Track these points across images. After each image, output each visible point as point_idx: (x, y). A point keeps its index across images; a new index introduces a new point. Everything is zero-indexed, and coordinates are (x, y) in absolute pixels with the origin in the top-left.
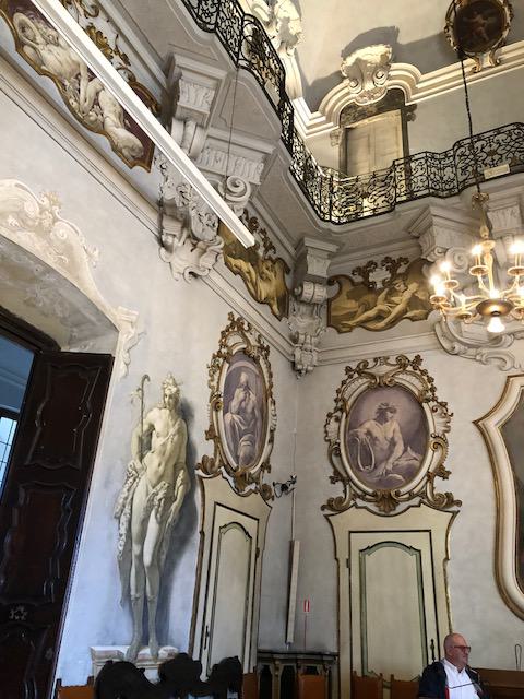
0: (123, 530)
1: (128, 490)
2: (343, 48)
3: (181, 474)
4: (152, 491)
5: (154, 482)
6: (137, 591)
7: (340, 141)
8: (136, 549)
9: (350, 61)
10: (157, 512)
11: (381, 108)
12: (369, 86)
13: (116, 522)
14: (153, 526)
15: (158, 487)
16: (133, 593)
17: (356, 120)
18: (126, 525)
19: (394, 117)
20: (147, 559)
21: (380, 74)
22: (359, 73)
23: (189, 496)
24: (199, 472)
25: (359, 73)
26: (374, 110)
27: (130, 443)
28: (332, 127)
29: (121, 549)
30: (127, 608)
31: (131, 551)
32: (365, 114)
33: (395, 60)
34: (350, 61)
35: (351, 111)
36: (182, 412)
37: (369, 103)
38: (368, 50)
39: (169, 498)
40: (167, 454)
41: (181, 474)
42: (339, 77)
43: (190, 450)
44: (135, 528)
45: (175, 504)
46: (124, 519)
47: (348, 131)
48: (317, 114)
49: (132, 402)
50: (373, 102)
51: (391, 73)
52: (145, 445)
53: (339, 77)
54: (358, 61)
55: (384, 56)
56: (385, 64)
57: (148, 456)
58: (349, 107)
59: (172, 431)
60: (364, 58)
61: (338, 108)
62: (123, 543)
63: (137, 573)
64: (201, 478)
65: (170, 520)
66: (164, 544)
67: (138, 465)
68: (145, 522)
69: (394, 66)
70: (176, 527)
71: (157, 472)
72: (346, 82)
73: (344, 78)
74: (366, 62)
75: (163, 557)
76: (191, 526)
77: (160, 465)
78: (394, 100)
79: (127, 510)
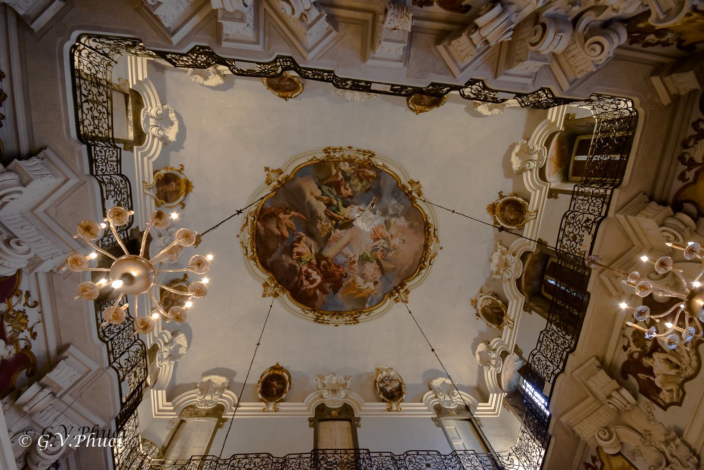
2: (205, 371)
7: (173, 427)
9: (205, 379)
11: (208, 414)
12: (208, 398)
17: (190, 416)
19: (213, 421)
21: (217, 393)
22: (206, 388)
25: (206, 388)
26: (204, 414)
28: (174, 416)
32: (197, 414)
33: (228, 388)
34: (205, 379)
35: (191, 409)
37: (203, 408)
38: (217, 377)
42: (194, 386)
47: (182, 421)
48: (170, 404)
50: (206, 408)
51: (224, 395)
53: (194, 386)
54: (209, 381)
55: (223, 384)
56: (222, 389)
58: (191, 406)
60: (213, 381)
61: (183, 406)
69: (227, 391)
72: (197, 390)
73: (197, 387)
74: (213, 383)
78: (218, 411)
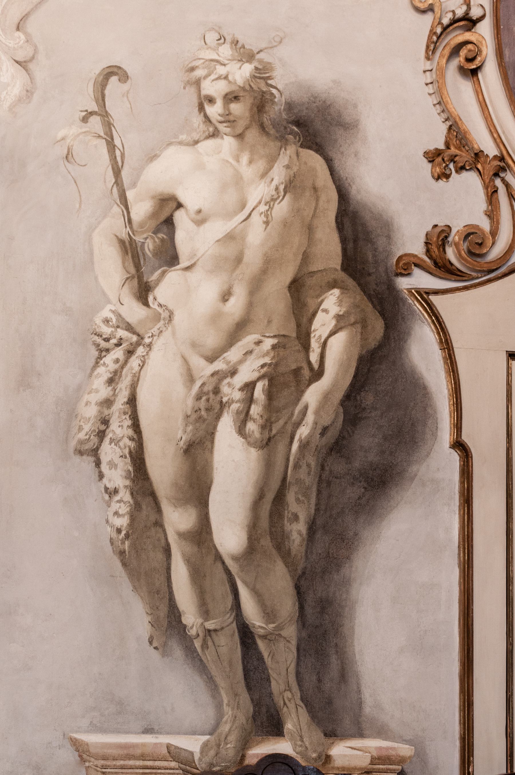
0: (117, 476)
1: (111, 381)
3: (331, 305)
4: (205, 370)
5: (212, 340)
6: (205, 613)
8: (178, 519)
10: (243, 420)
13: (86, 463)
14: (235, 465)
15: (234, 355)
16: (191, 617)
18: (125, 466)
20: (230, 536)
23: (378, 365)
24: (421, 280)
27: (89, 263)
29: (123, 522)
30: (178, 652)
31: (159, 524)
36: (309, 128)
39: (286, 379)
40: (253, 258)
41: (331, 305)
43: (358, 232)
44: (164, 468)
45: (312, 395)
46: (108, 452)
49: (68, 156)
52: (152, 249)
57: (168, 287)
59: (258, 192)
62: (124, 509)
63: (197, 575)
64: (424, 295)
65: (303, 431)
66: (291, 497)
67: (134, 311)
68: (197, 451)
70: (337, 445)
71: (215, 318)
75: (297, 531)
76: (407, 432)
77: (225, 296)
79: (120, 428)
